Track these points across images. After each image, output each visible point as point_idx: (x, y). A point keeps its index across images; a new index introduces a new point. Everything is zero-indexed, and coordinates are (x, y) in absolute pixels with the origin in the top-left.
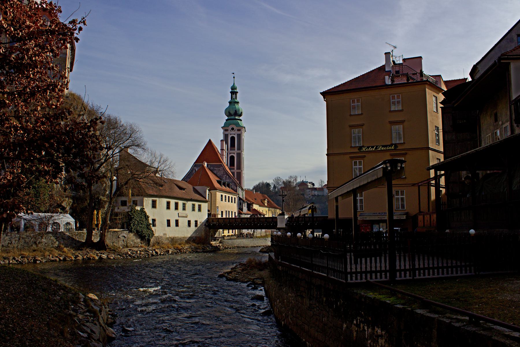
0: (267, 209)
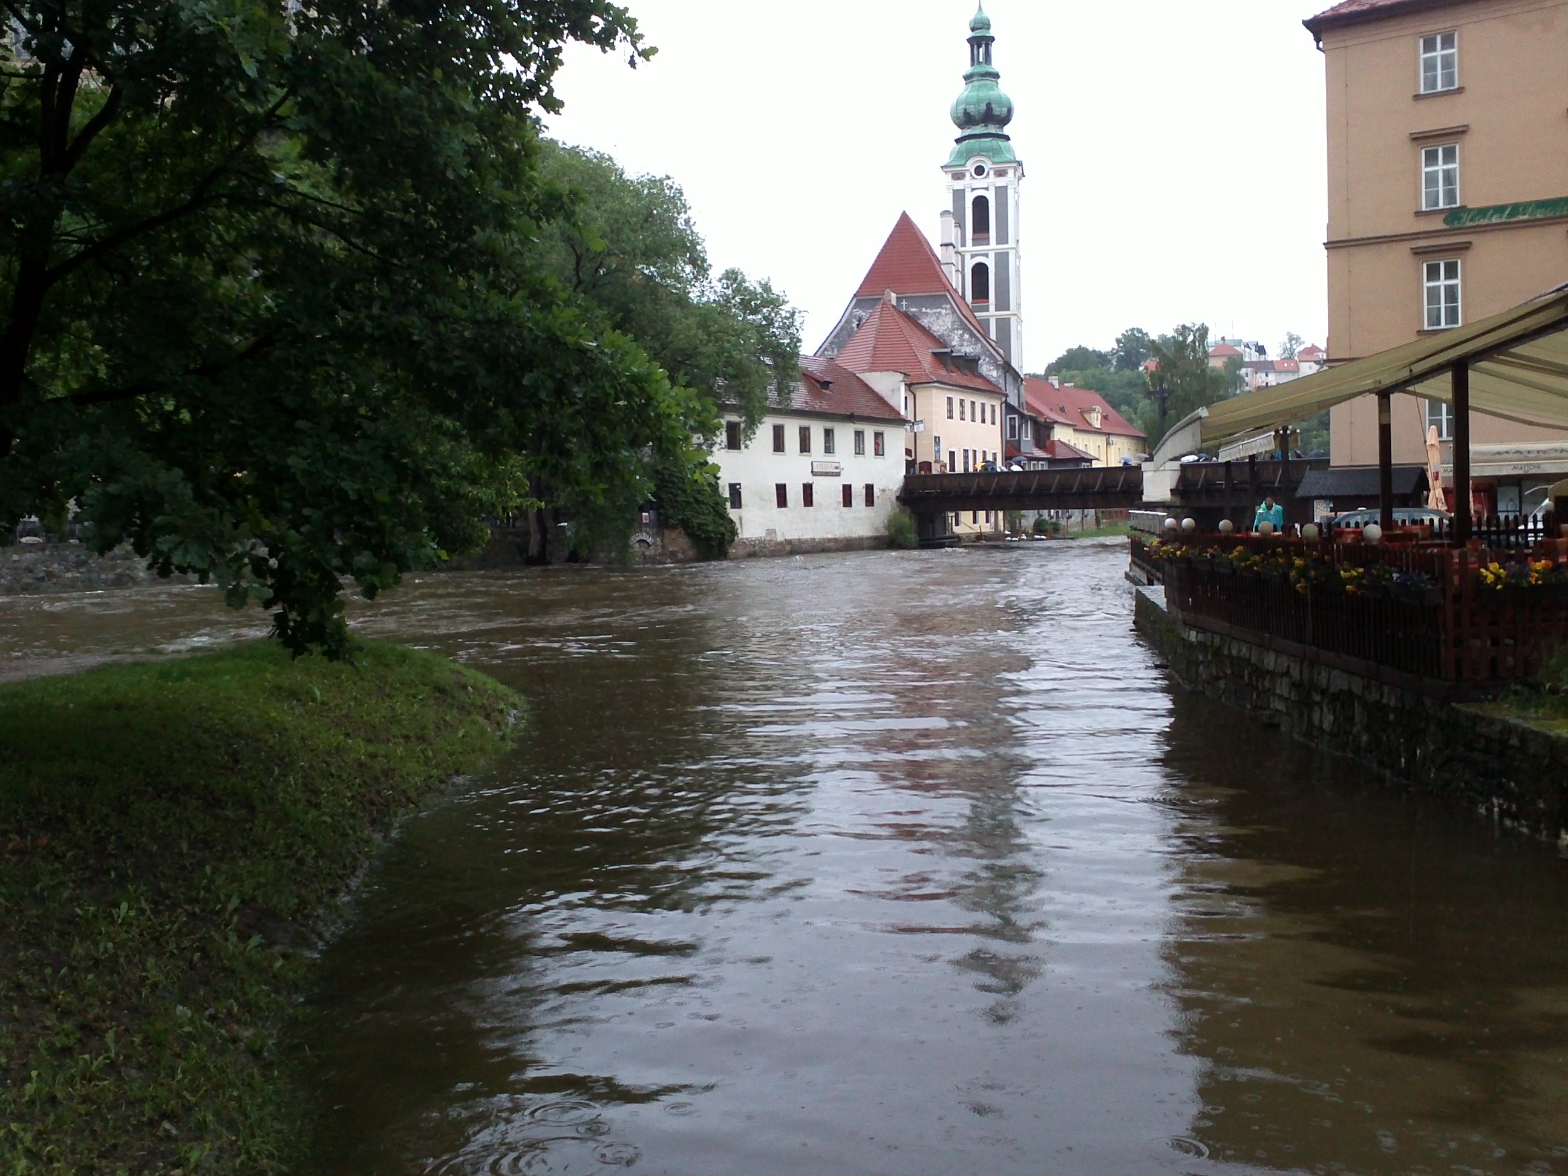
0: (1101, 440)
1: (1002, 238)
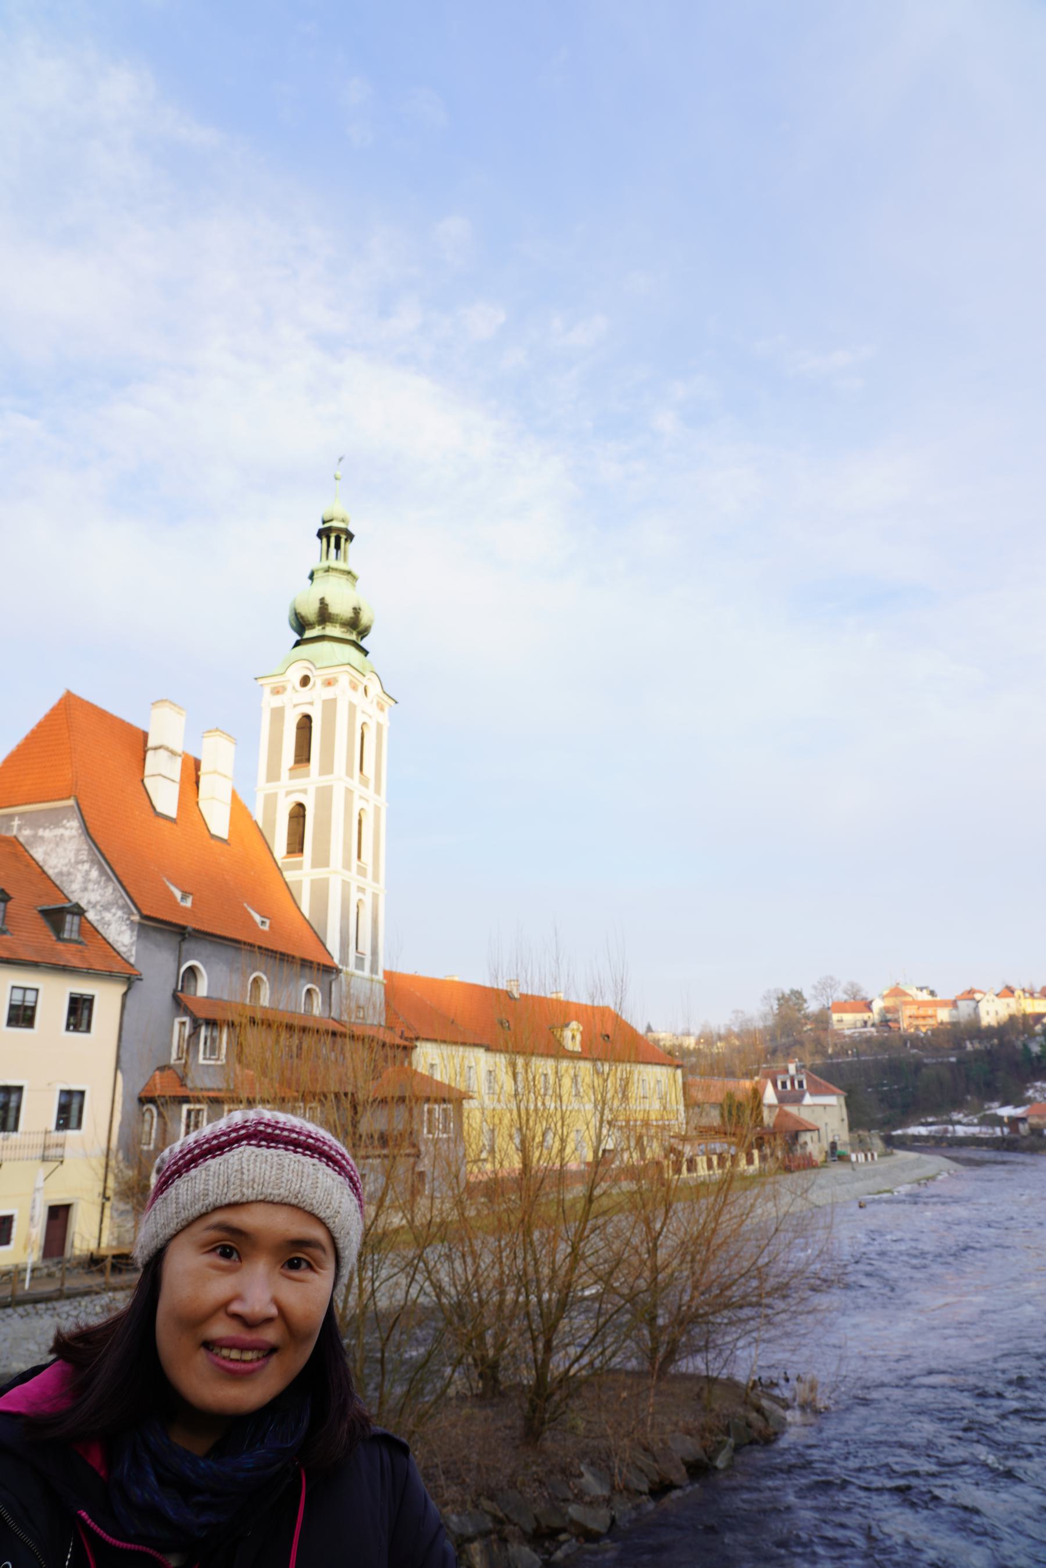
1: (327, 768)
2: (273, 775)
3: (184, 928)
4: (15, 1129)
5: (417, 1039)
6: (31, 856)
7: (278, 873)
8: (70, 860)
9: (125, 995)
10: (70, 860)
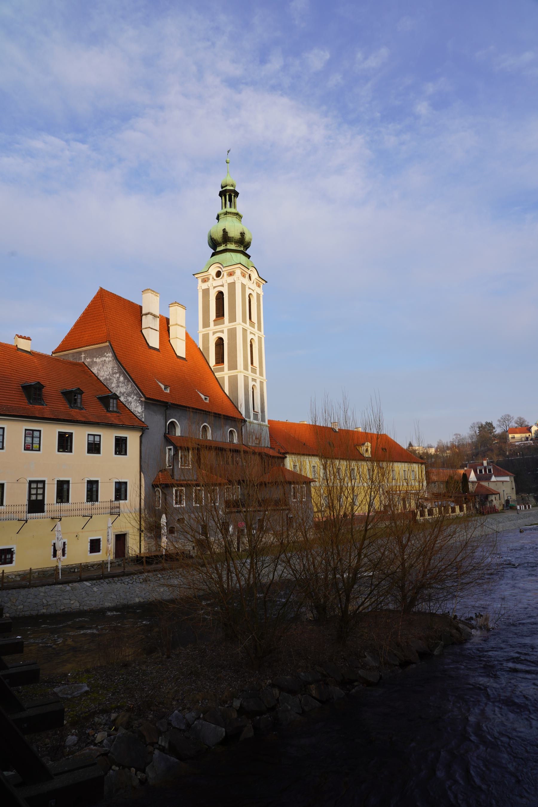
1: (233, 319)
2: (206, 324)
3: (167, 403)
4: (97, 500)
5: (287, 453)
6: (92, 371)
7: (212, 374)
8: (110, 372)
9: (141, 437)
10: (110, 372)
